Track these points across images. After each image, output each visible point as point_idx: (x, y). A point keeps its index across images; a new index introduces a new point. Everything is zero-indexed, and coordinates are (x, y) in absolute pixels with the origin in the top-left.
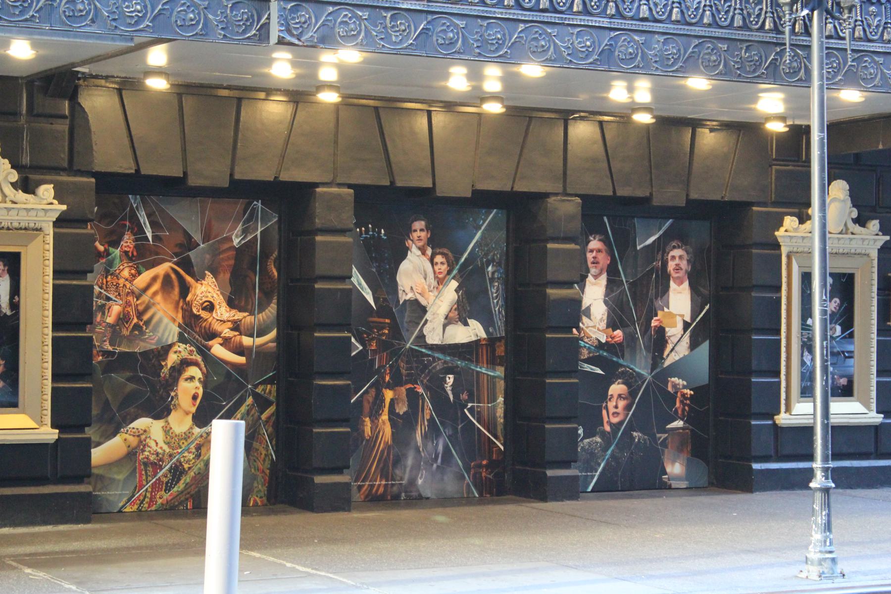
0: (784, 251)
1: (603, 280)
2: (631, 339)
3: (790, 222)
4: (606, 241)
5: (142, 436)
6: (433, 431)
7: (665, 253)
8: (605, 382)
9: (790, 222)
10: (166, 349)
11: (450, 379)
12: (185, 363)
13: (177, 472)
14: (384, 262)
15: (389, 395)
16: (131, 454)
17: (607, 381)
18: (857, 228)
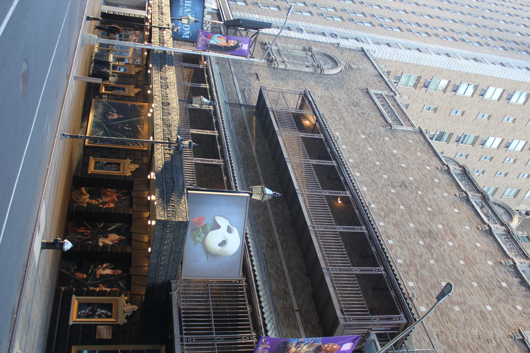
0: (119, 298)
1: (111, 273)
2: (97, 279)
3: (126, 298)
4: (121, 274)
5: (86, 195)
6: (79, 239)
7: (118, 288)
8: (87, 273)
9: (126, 298)
10: (101, 199)
11: (91, 242)
12: (99, 201)
13: (78, 199)
14: (116, 231)
15: (89, 232)
16: (82, 194)
17: (87, 274)
18: (125, 316)
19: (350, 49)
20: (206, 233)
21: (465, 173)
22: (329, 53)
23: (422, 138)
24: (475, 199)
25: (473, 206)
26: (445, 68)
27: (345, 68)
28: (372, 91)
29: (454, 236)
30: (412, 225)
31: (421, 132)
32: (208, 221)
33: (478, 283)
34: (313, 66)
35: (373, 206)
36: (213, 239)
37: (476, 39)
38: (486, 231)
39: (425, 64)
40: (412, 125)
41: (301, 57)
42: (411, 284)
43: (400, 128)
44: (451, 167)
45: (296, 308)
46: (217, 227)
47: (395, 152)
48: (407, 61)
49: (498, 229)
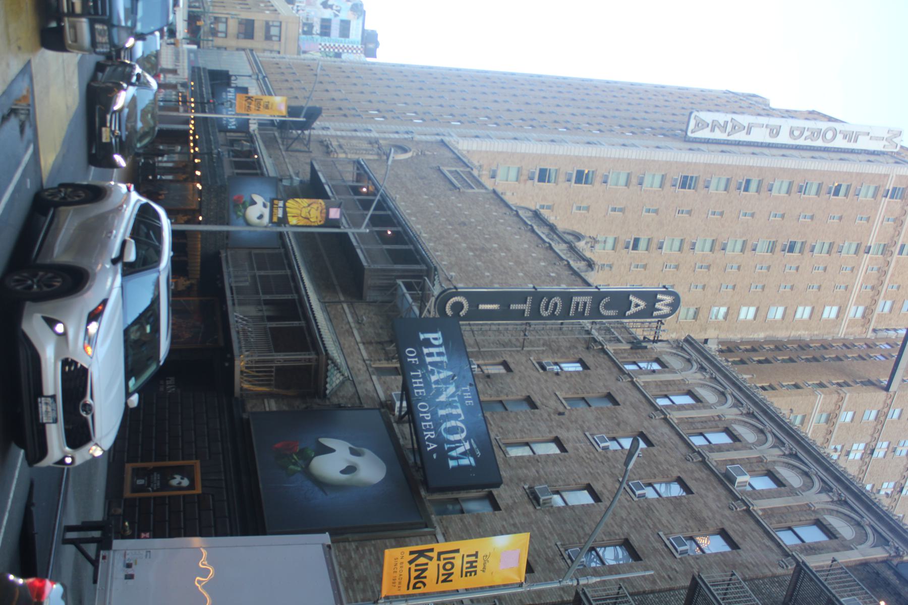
19: (427, 142)
20: (245, 208)
21: (536, 215)
22: (399, 144)
23: (495, 197)
24: (542, 231)
25: (537, 234)
26: (548, 152)
27: (417, 154)
28: (445, 170)
29: (509, 250)
30: (464, 245)
31: (494, 192)
32: (246, 198)
33: (525, 274)
34: (378, 154)
35: (424, 235)
36: (253, 213)
37: (598, 127)
38: (547, 248)
39: (523, 151)
40: (486, 189)
41: (366, 150)
42: (453, 274)
43: (470, 191)
44: (521, 212)
45: (336, 282)
46: (254, 203)
47: (460, 205)
48: (500, 150)
49: (560, 248)
